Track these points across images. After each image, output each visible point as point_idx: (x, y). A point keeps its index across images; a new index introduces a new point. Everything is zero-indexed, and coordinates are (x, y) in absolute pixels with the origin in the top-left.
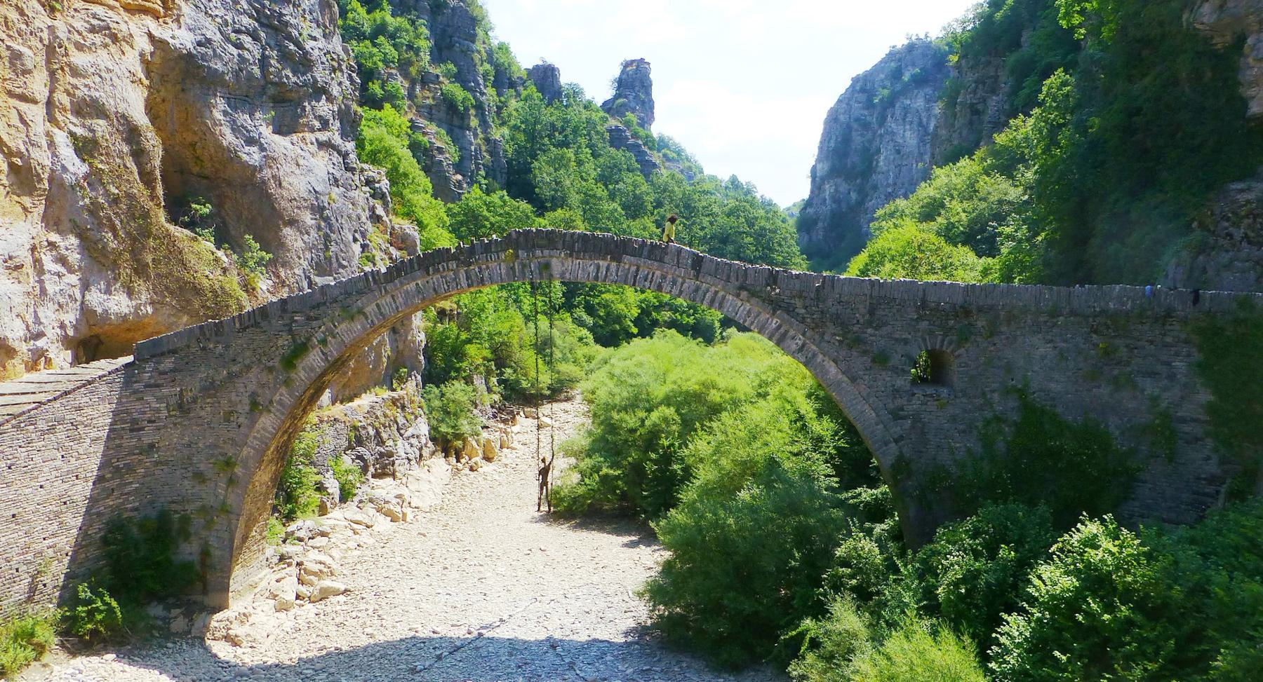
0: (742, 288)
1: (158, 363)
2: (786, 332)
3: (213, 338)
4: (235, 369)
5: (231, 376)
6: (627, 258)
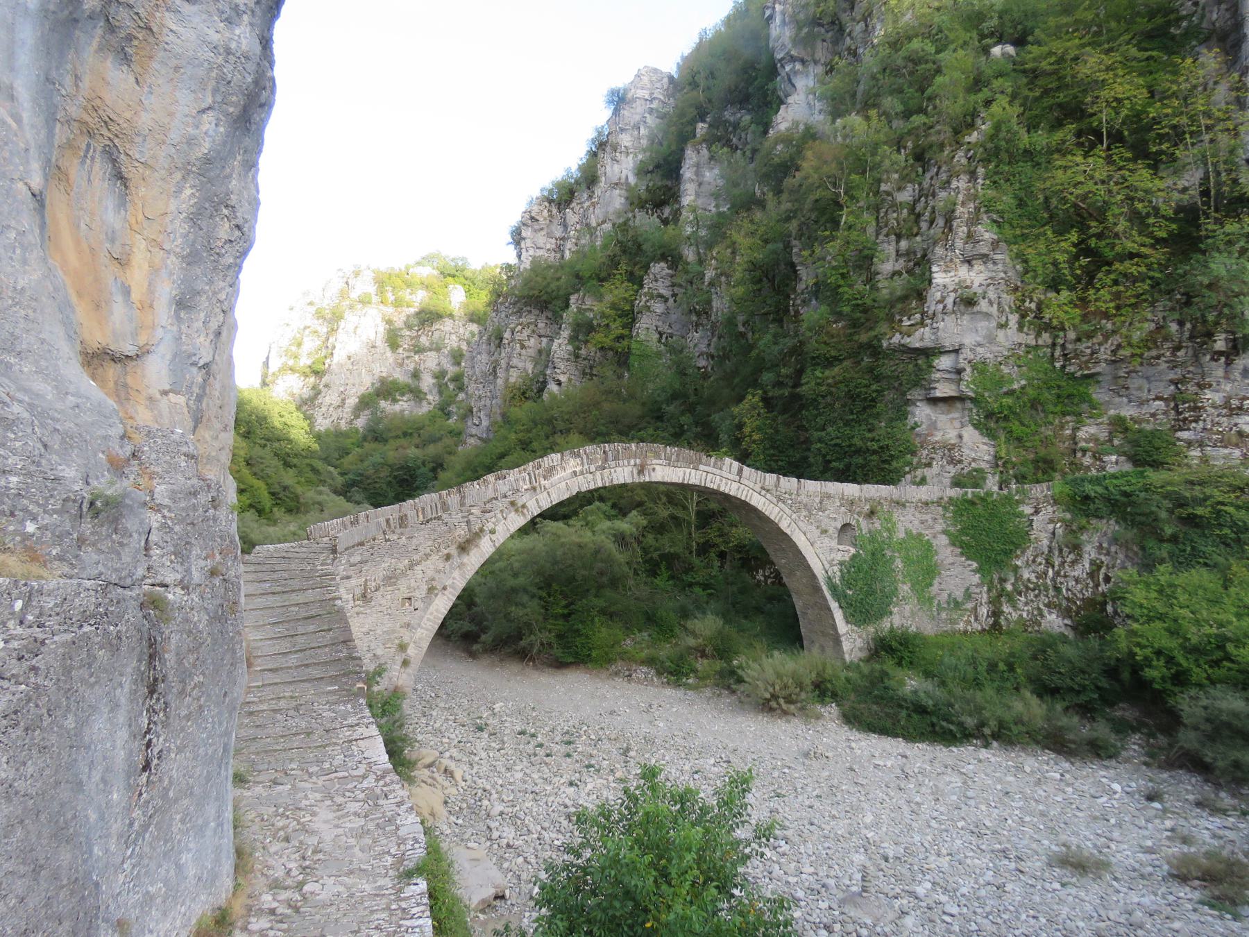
0: (762, 488)
1: (350, 555)
3: (398, 531)
4: (416, 557)
5: (411, 566)
6: (702, 467)
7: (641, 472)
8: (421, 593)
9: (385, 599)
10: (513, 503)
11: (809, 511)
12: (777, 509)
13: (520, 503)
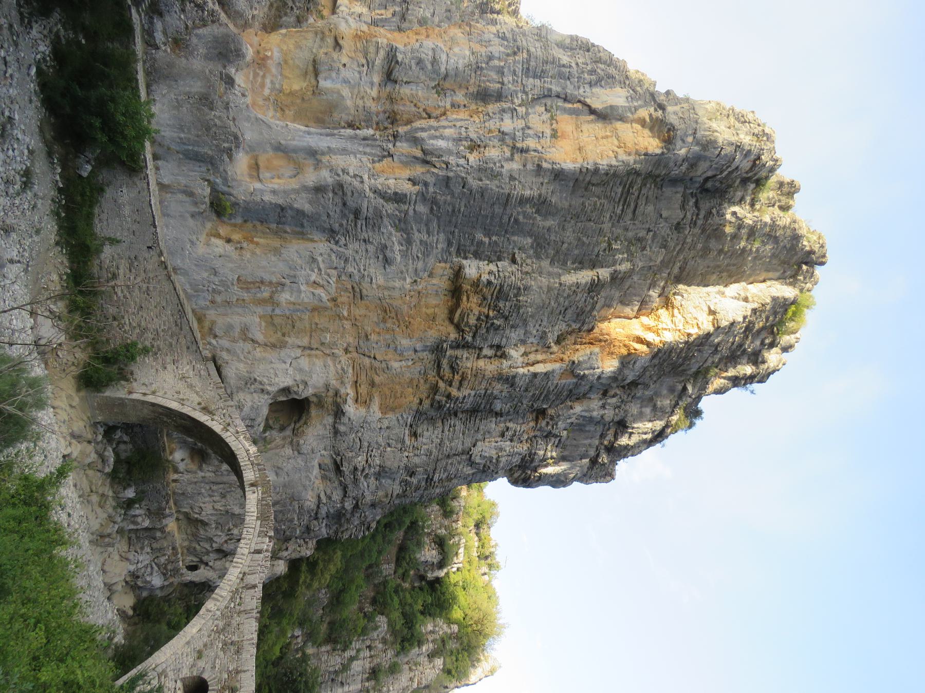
2: (219, 601)
5: (197, 393)
6: (259, 522)
7: (252, 485)
8: (181, 396)
9: (181, 386)
10: (229, 425)
11: (224, 629)
12: (224, 594)
13: (229, 428)
